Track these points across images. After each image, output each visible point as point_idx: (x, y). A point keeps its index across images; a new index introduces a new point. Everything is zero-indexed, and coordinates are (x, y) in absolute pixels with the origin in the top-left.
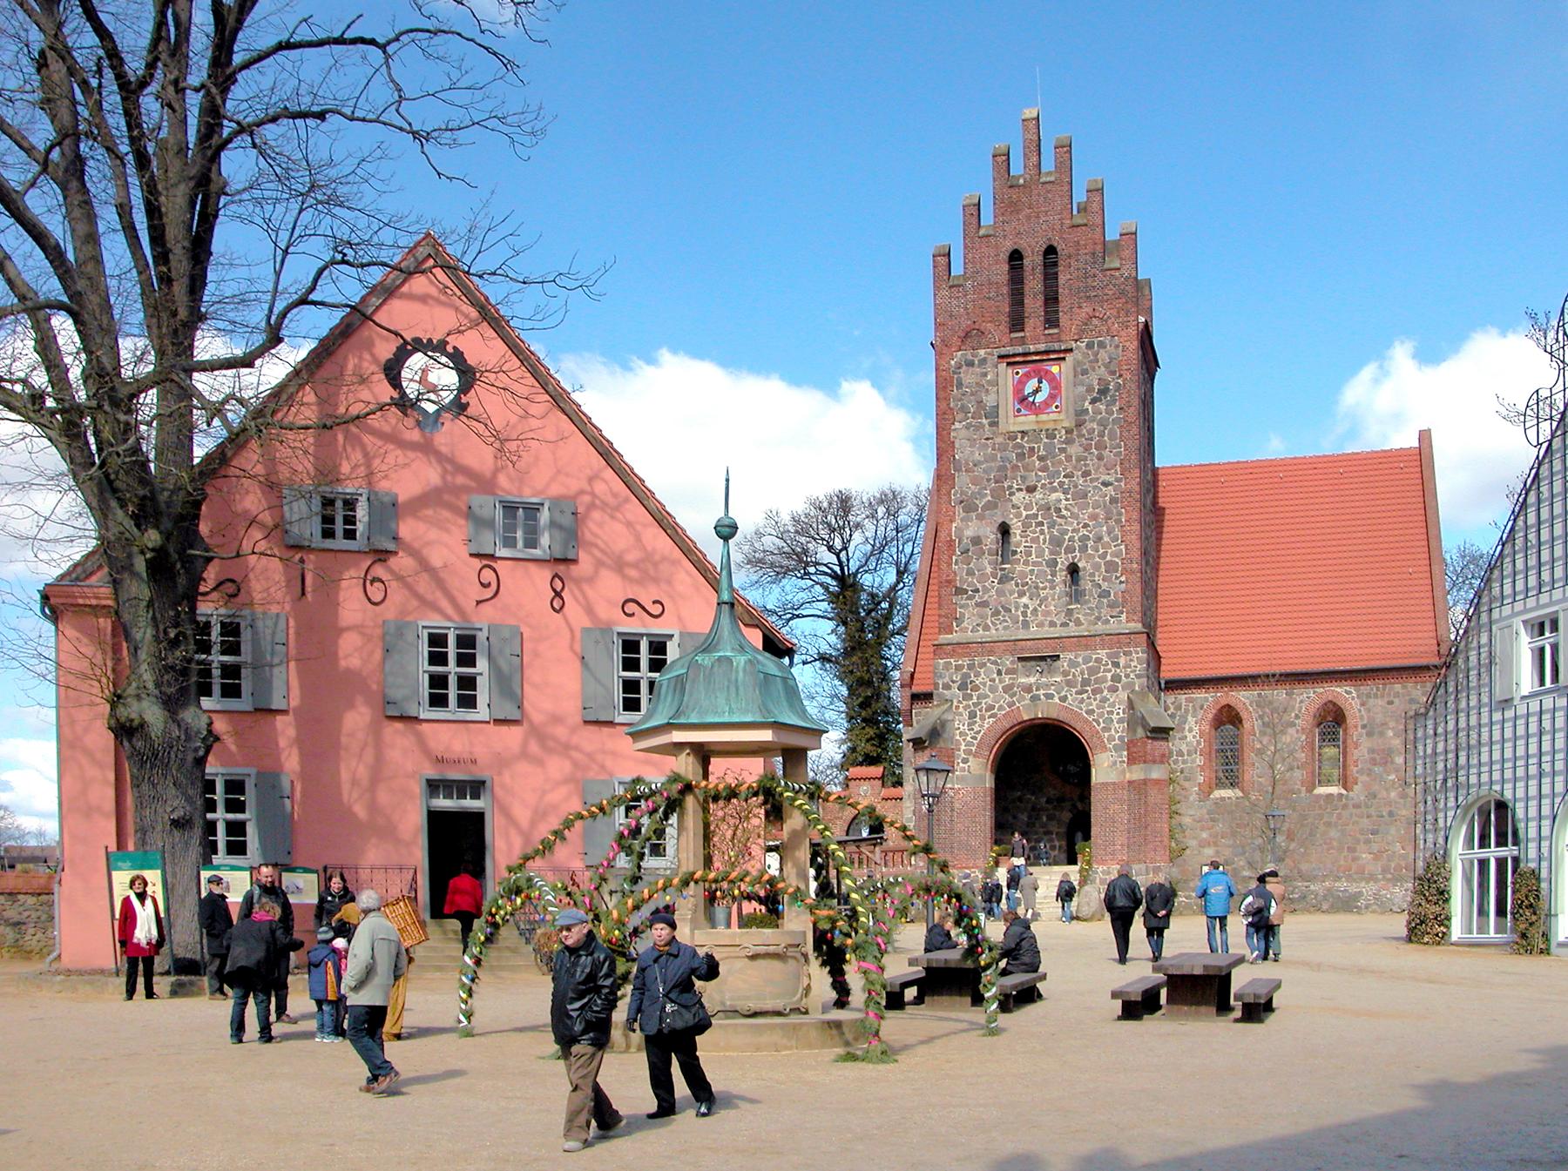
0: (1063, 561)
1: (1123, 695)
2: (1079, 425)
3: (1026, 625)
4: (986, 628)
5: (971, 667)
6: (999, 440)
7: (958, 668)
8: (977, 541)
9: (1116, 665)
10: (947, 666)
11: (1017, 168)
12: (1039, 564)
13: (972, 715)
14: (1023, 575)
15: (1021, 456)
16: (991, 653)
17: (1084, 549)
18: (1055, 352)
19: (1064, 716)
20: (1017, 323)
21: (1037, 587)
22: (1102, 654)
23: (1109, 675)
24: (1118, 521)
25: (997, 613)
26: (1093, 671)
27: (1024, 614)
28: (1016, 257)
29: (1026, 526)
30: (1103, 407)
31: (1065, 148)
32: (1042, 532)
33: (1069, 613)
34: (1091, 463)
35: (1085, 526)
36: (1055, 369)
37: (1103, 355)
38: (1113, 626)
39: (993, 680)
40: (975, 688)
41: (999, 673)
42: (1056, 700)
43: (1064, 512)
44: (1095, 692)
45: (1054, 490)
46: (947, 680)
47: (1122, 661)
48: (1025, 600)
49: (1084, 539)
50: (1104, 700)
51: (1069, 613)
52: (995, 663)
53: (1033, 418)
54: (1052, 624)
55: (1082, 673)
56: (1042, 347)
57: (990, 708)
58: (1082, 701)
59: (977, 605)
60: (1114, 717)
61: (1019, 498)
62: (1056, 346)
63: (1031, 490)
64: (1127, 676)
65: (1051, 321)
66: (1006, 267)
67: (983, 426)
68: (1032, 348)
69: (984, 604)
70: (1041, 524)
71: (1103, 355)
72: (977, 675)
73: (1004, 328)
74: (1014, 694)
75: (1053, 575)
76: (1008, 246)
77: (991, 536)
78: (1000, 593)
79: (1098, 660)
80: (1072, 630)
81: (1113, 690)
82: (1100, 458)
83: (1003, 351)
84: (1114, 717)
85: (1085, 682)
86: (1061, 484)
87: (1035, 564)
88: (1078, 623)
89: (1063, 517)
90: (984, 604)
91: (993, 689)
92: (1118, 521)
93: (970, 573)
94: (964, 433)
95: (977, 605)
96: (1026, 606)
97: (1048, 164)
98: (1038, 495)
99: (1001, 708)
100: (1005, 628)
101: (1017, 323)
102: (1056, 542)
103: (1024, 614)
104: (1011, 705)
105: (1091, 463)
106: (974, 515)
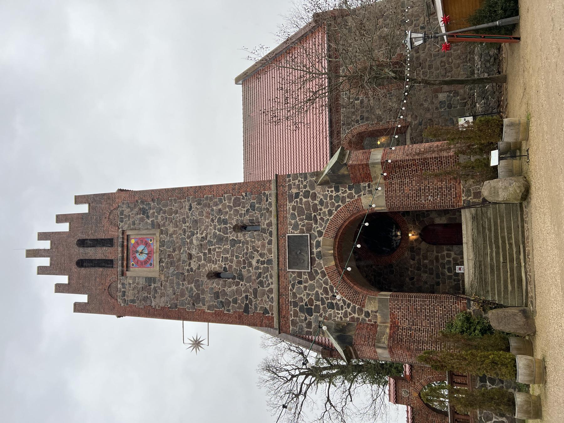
0: (232, 236)
1: (318, 189)
2: (159, 226)
3: (270, 262)
4: (271, 291)
5: (295, 304)
6: (163, 277)
7: (296, 314)
8: (217, 295)
9: (297, 195)
10: (294, 323)
11: (45, 262)
12: (233, 251)
13: (331, 306)
14: (239, 262)
15: (172, 263)
16: (286, 288)
17: (225, 222)
18: (123, 242)
19: (332, 234)
20: (108, 263)
21: (247, 254)
22: (289, 206)
23: (304, 200)
24: (211, 199)
25: (261, 283)
26: (301, 212)
27: (263, 263)
28: (81, 263)
29: (210, 261)
30: (151, 211)
31: (42, 236)
32: (214, 249)
33: (264, 231)
34: (179, 217)
35: (213, 220)
36: (133, 241)
37: (127, 211)
38: (273, 200)
39: (305, 287)
40: (311, 301)
41: (300, 282)
42: (321, 239)
43: (204, 235)
44: (315, 210)
45: (191, 242)
46: (304, 325)
47: (294, 191)
48: (254, 262)
49: (220, 221)
50: (321, 203)
51: (264, 231)
52: (293, 286)
53: (155, 255)
54: (270, 243)
55: (301, 220)
56: (120, 249)
57: (326, 291)
58: (322, 219)
59: (256, 297)
60: (334, 194)
61: (194, 266)
62: (120, 240)
63: (190, 256)
64: (305, 187)
65: (109, 242)
66: (83, 269)
67: (155, 288)
68: (120, 255)
69: (255, 292)
70: (210, 250)
71: (127, 211)
72: (301, 300)
73: (109, 271)
74: (316, 272)
75: (240, 242)
76: (75, 268)
77: (216, 285)
78: (249, 280)
79: (294, 208)
80: (274, 229)
81: (314, 197)
82: (176, 212)
83: (119, 273)
84: (334, 194)
85: (309, 218)
86: (189, 237)
87: (232, 255)
88: (270, 224)
89: (206, 236)
90: (255, 292)
91: (312, 288)
92: (211, 199)
93: (235, 301)
94: (157, 300)
95: (256, 297)
96: (258, 262)
97: (46, 245)
98: (194, 252)
99: (326, 283)
100: (271, 278)
101: (108, 263)
102: (220, 240)
103: (263, 263)
104: (324, 275)
105: (179, 217)
106: (201, 296)
